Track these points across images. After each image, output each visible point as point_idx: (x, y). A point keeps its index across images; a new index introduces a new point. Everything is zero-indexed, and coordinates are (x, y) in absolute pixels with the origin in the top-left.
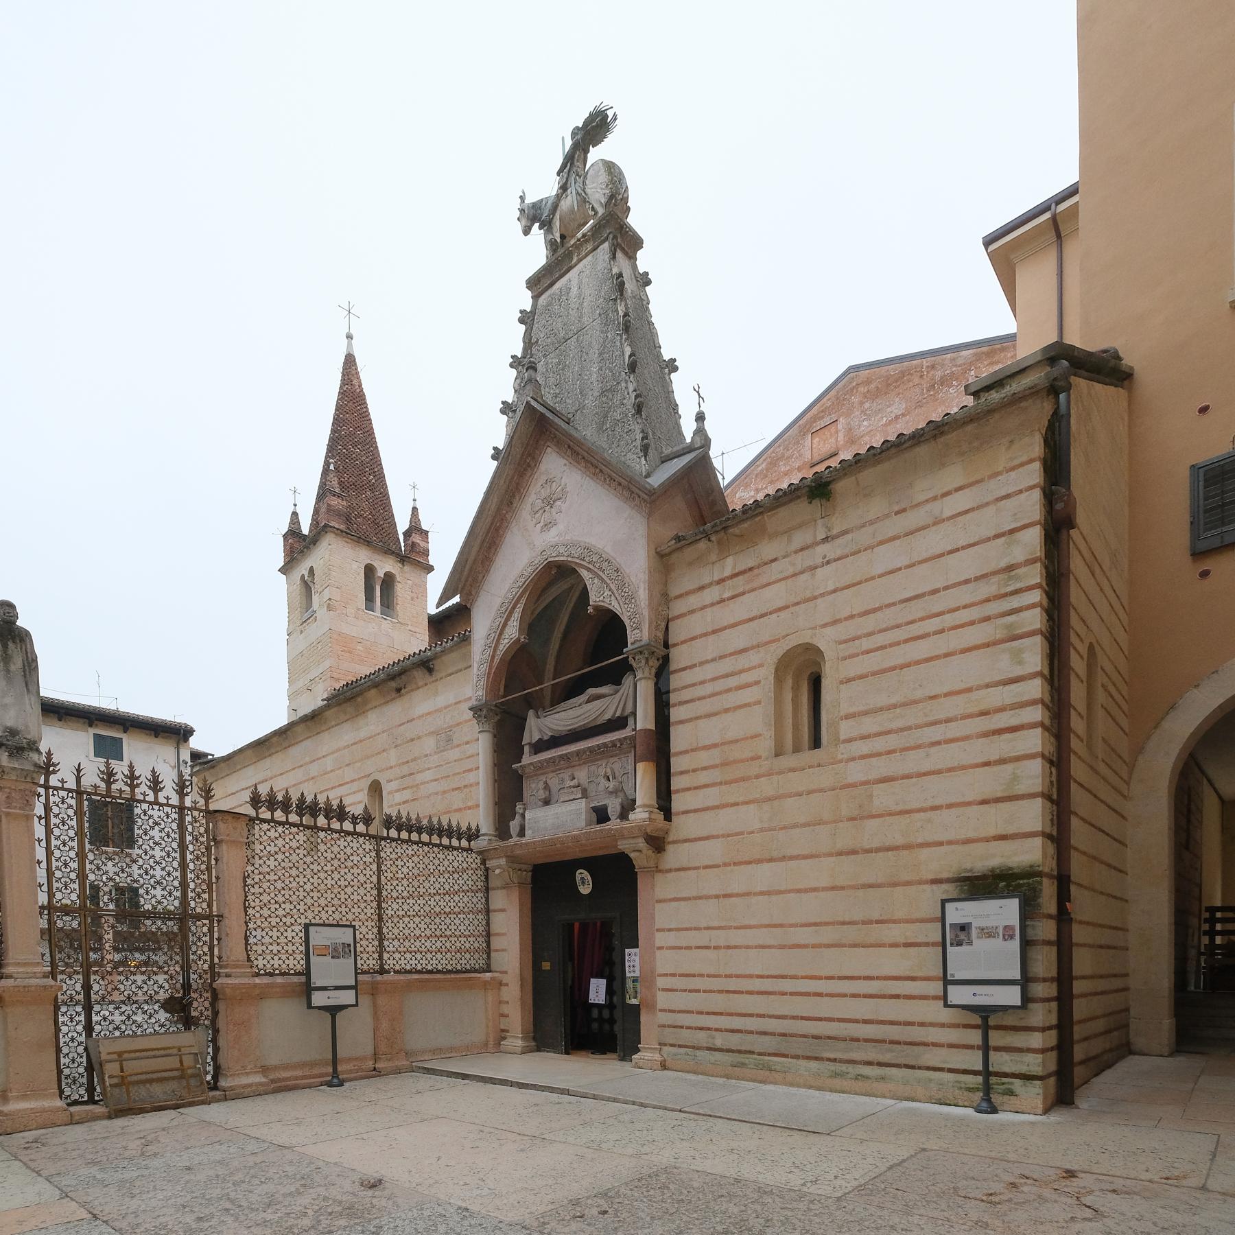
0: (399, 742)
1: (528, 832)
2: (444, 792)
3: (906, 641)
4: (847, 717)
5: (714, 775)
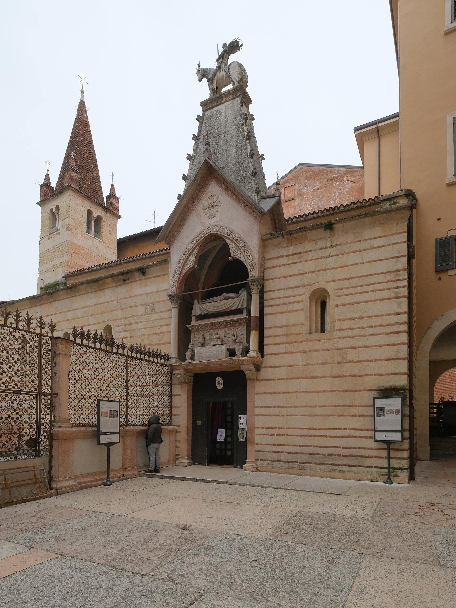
0: (124, 307)
1: (196, 358)
2: (149, 335)
3: (360, 293)
4: (338, 320)
5: (284, 339)
